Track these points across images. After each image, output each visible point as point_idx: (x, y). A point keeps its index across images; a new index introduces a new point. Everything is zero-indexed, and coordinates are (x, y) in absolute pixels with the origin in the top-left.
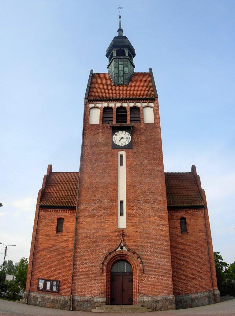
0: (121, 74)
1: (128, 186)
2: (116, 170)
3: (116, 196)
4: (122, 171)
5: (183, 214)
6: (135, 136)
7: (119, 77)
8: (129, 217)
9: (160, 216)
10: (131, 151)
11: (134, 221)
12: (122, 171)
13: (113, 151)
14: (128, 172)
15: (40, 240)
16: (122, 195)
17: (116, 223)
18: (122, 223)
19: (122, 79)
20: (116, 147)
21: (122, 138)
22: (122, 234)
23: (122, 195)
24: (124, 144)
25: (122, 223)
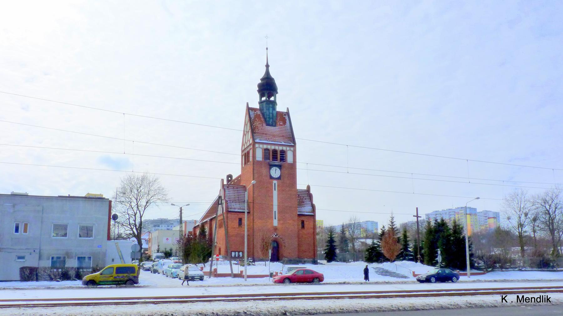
0: (271, 115)
1: (279, 202)
2: (272, 193)
3: (273, 208)
4: (275, 193)
5: (303, 218)
6: (282, 170)
7: (269, 118)
8: (279, 220)
9: (294, 221)
10: (280, 181)
11: (281, 222)
12: (275, 193)
13: (271, 180)
14: (278, 194)
15: (230, 231)
16: (275, 208)
17: (272, 223)
18: (275, 223)
19: (271, 120)
20: (271, 178)
21: (275, 172)
22: (276, 229)
23: (275, 208)
24: (277, 177)
25: (275, 223)
